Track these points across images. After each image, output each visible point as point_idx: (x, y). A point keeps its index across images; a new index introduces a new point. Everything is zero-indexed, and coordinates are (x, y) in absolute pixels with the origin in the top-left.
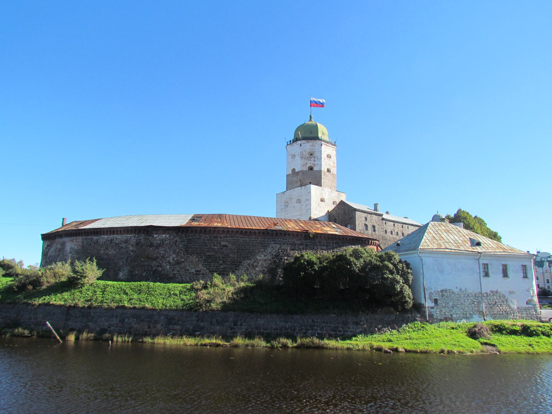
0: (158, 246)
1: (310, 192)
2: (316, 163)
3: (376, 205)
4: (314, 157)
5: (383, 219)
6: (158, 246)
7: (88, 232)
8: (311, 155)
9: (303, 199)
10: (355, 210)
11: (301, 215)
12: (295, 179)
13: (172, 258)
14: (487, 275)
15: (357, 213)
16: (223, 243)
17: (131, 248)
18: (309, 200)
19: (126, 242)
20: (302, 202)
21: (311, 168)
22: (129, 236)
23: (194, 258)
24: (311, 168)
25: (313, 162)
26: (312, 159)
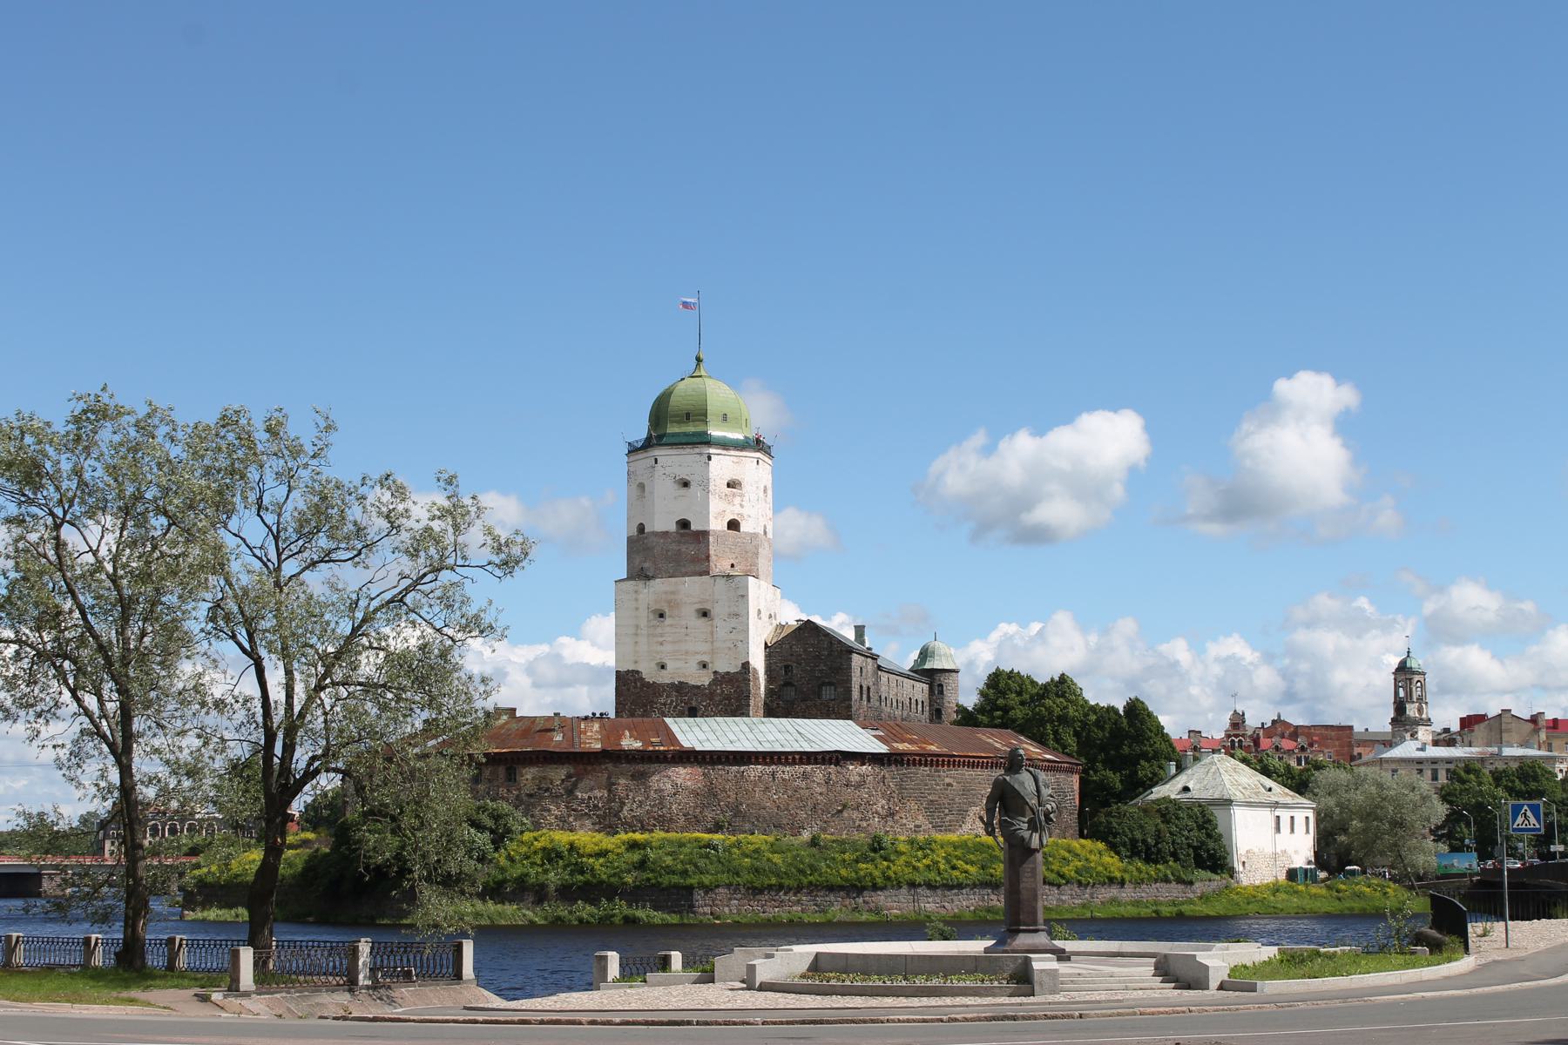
0: (859, 786)
1: (744, 597)
2: (745, 511)
3: (860, 631)
4: (742, 495)
5: (879, 668)
6: (859, 786)
7: (719, 758)
8: (729, 485)
9: (718, 611)
10: (850, 651)
11: (713, 652)
12: (690, 549)
13: (881, 805)
14: (1278, 829)
15: (855, 657)
16: (947, 780)
17: (818, 790)
18: (739, 615)
19: (805, 776)
20: (717, 622)
21: (733, 525)
22: (809, 768)
23: (913, 805)
24: (733, 525)
25: (737, 509)
26: (737, 500)
